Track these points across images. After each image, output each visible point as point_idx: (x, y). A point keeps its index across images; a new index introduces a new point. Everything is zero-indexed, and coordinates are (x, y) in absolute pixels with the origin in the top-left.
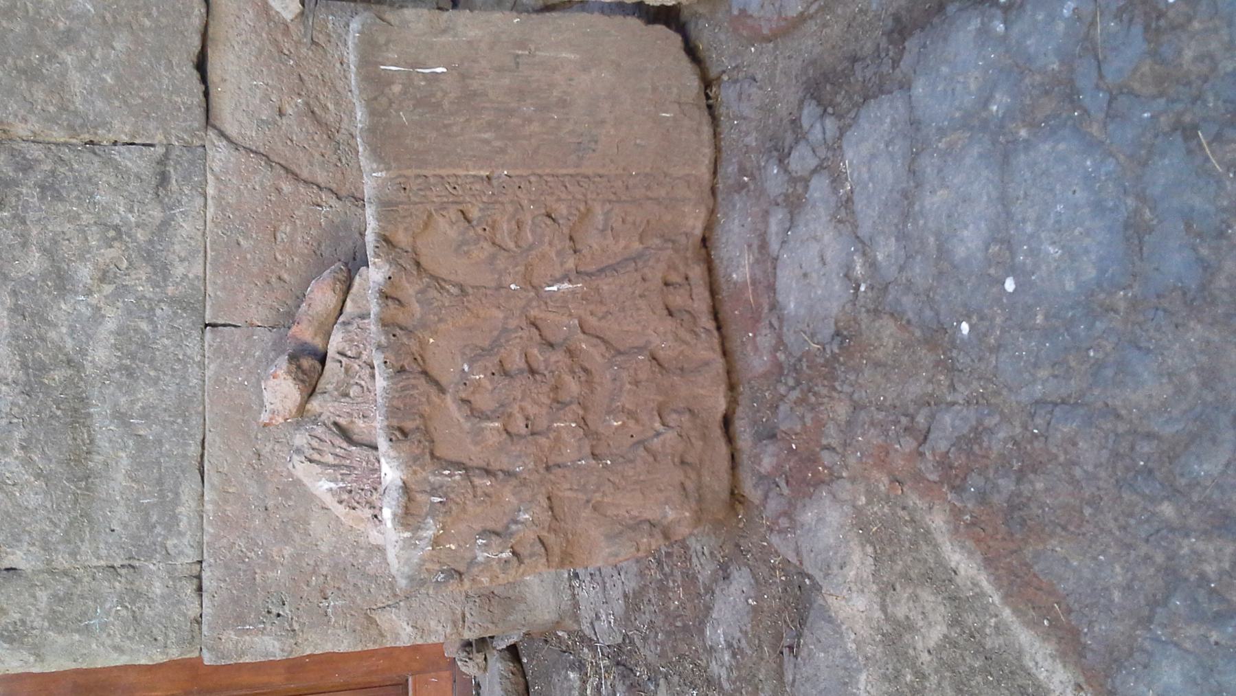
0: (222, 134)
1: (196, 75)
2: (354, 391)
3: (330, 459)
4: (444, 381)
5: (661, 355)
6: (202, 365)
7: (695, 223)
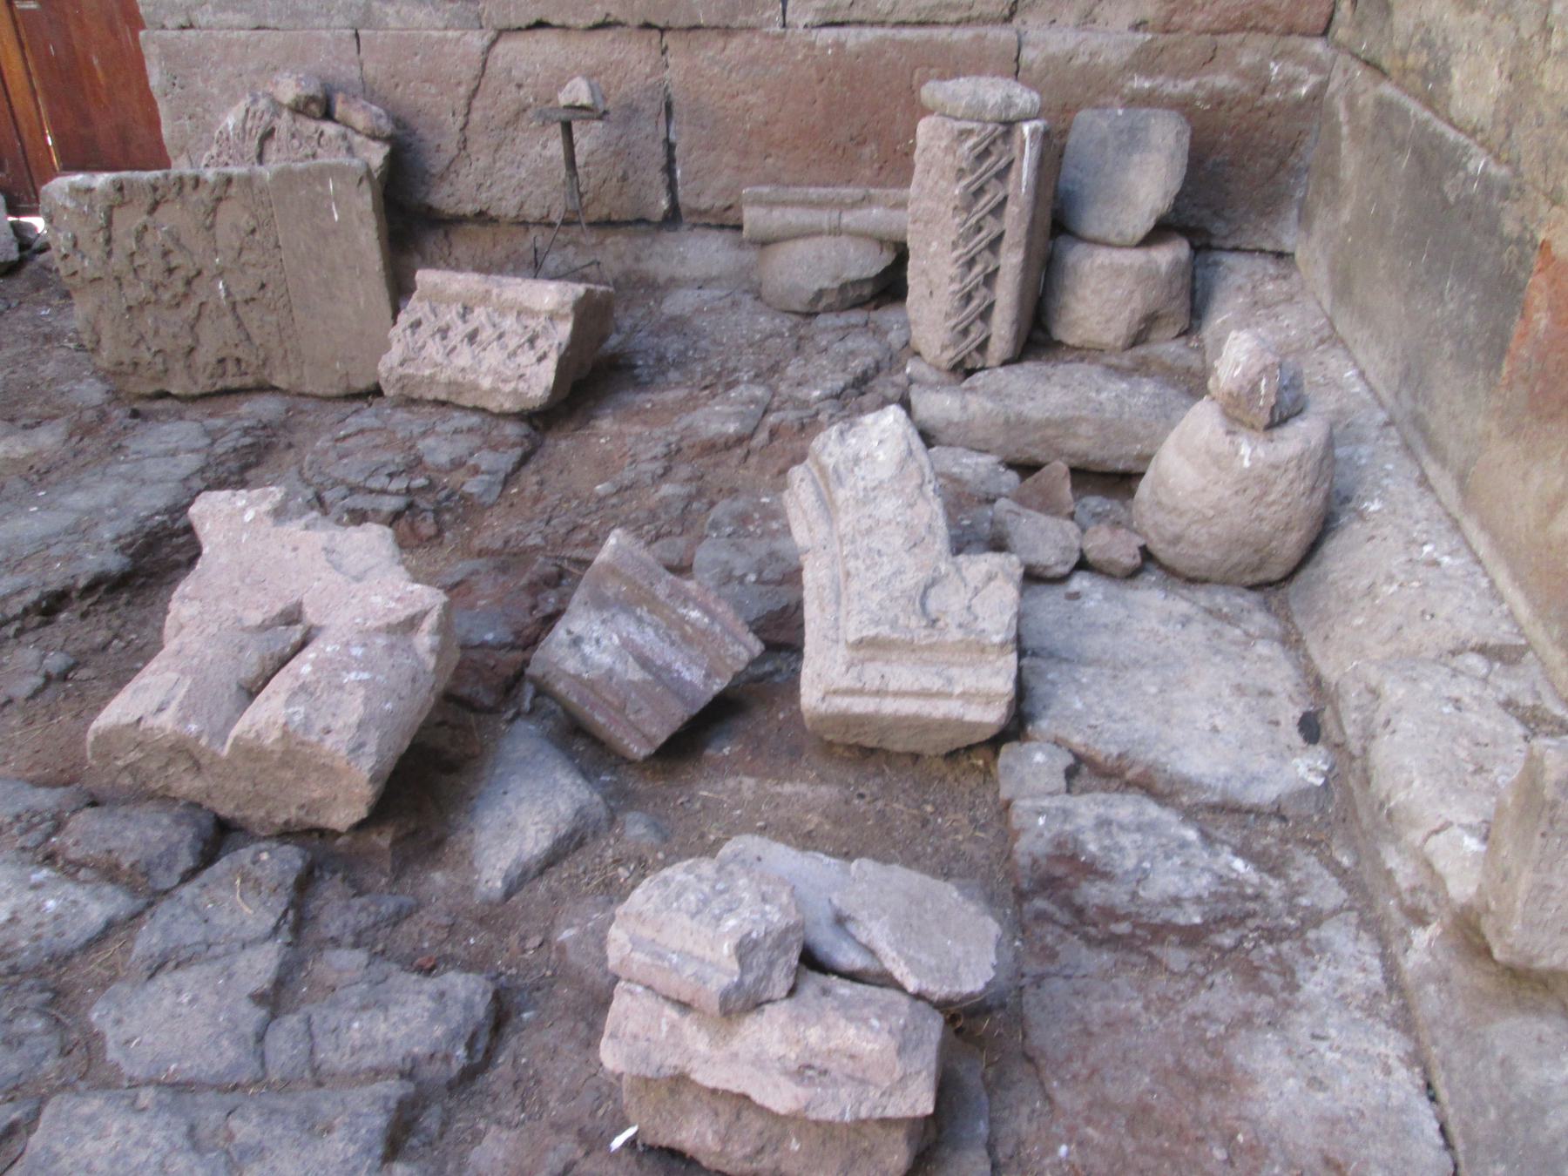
0: (494, 43)
1: (533, 21)
2: (296, 143)
3: (249, 125)
4: (156, 214)
5: (195, 354)
6: (328, 28)
7: (279, 380)
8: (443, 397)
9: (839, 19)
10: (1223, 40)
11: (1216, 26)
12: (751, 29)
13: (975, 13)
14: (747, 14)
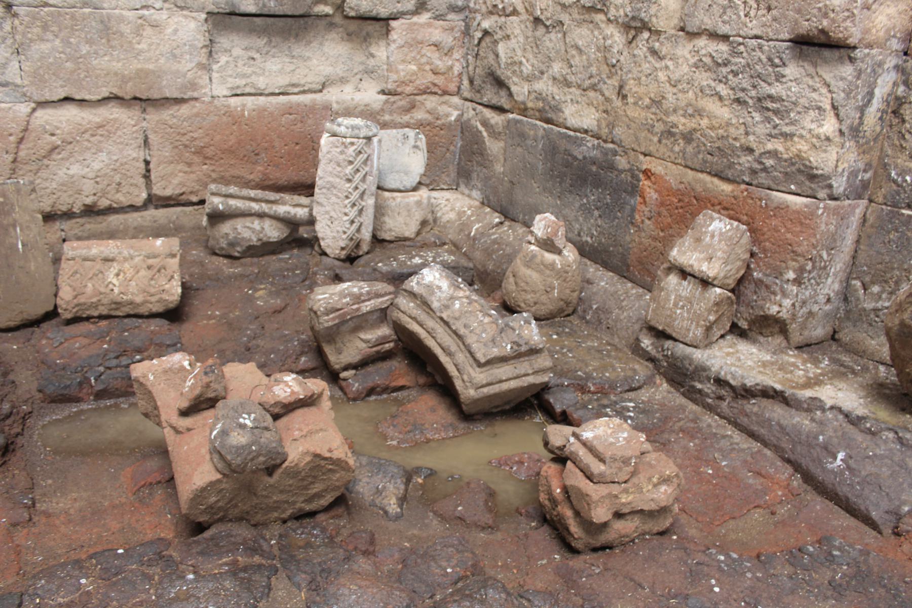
0: (34, 110)
1: (62, 97)
8: (105, 312)
9: (239, 92)
10: (418, 98)
11: (415, 92)
12: (196, 99)
13: (306, 88)
14: (193, 91)
